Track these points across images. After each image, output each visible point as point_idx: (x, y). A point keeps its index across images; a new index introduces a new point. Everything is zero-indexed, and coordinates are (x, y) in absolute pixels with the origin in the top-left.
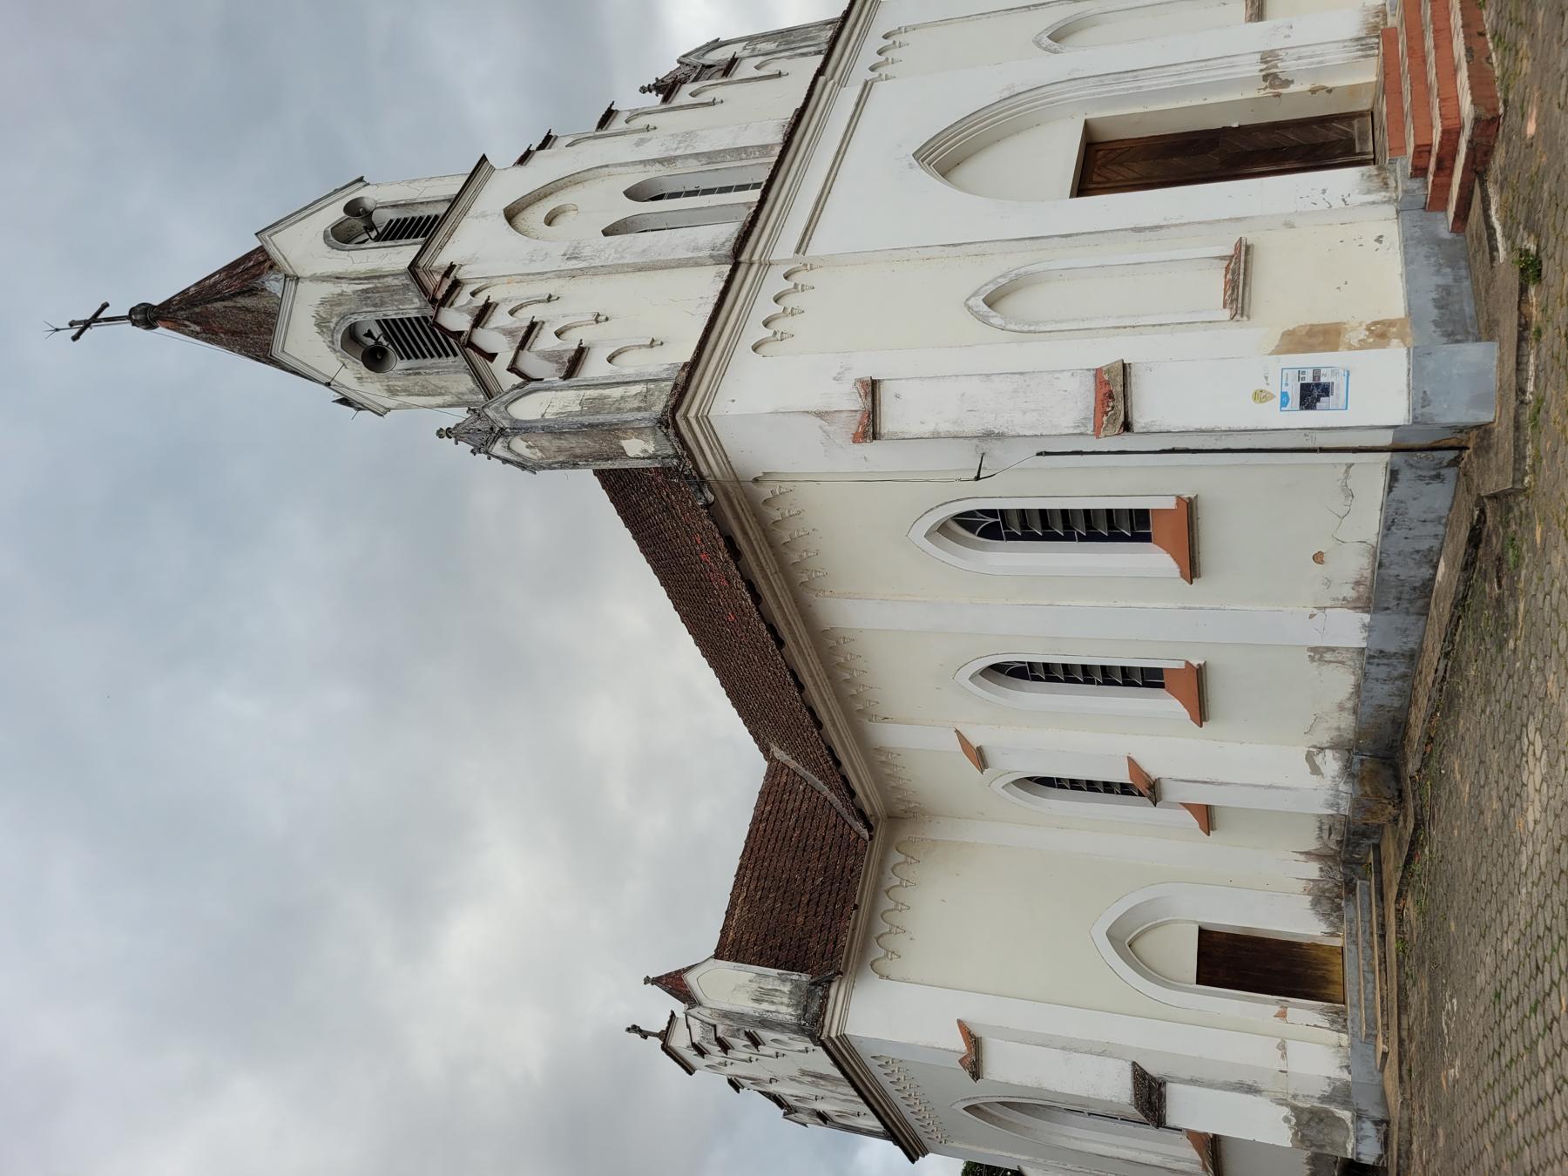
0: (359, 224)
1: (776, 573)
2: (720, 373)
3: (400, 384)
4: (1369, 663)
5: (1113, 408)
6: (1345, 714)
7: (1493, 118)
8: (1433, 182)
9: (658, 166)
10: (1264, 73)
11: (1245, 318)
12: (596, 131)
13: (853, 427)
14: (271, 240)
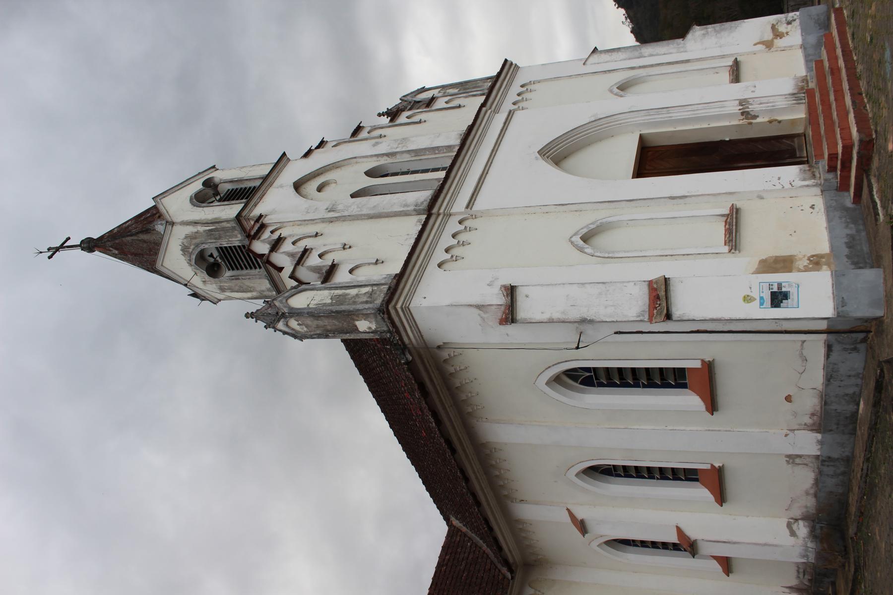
0: (210, 192)
1: (451, 406)
2: (417, 280)
3: (227, 285)
4: (823, 465)
5: (660, 305)
6: (810, 497)
7: (870, 140)
8: (840, 174)
9: (385, 158)
10: (741, 111)
11: (737, 252)
12: (351, 138)
13: (500, 315)
14: (161, 201)
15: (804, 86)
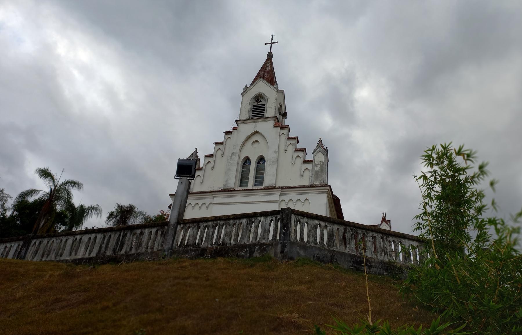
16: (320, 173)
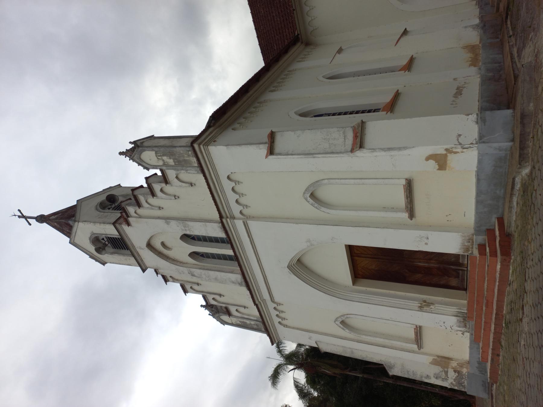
15: (469, 246)
16: (177, 157)
